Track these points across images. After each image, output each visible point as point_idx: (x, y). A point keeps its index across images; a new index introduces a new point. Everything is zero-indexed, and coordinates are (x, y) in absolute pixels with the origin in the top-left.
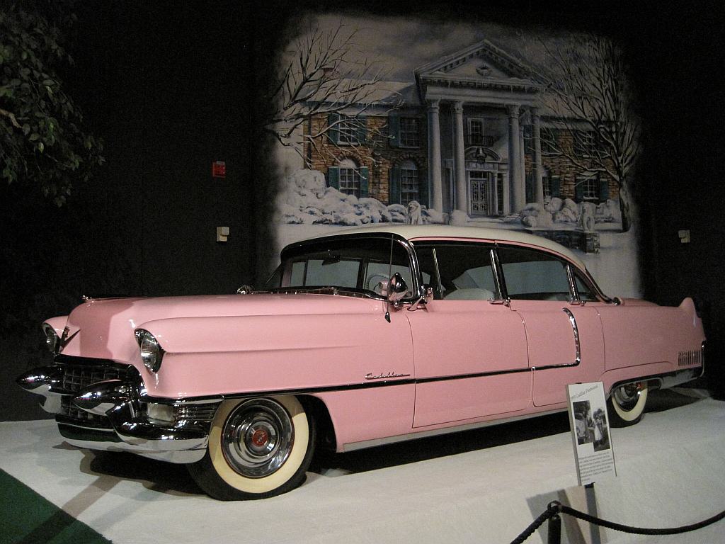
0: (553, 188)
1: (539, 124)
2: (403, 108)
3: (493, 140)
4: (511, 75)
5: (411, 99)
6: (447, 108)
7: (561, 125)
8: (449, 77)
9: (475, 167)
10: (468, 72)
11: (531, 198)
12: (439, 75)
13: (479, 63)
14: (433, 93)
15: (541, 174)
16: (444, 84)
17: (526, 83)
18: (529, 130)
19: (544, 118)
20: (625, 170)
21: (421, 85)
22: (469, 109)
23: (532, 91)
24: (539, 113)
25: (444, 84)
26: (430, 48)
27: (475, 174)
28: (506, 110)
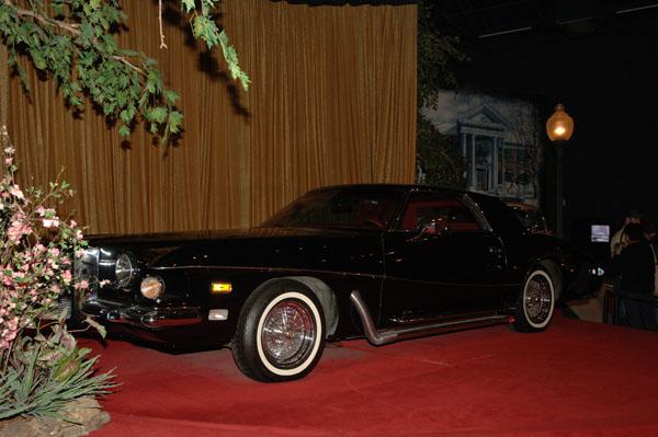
0: (509, 178)
1: (505, 147)
2: (451, 137)
3: (486, 154)
4: (493, 121)
5: (455, 132)
6: (469, 137)
7: (513, 147)
8: (470, 122)
9: (478, 166)
10: (477, 120)
11: (500, 182)
12: (466, 121)
13: (482, 116)
14: (464, 130)
15: (504, 170)
16: (468, 125)
17: (499, 126)
18: (500, 149)
19: (507, 144)
20: (537, 169)
21: (459, 125)
22: (478, 138)
23: (502, 130)
24: (505, 141)
25: (468, 125)
26: (464, 107)
27: (479, 170)
28: (491, 139)
